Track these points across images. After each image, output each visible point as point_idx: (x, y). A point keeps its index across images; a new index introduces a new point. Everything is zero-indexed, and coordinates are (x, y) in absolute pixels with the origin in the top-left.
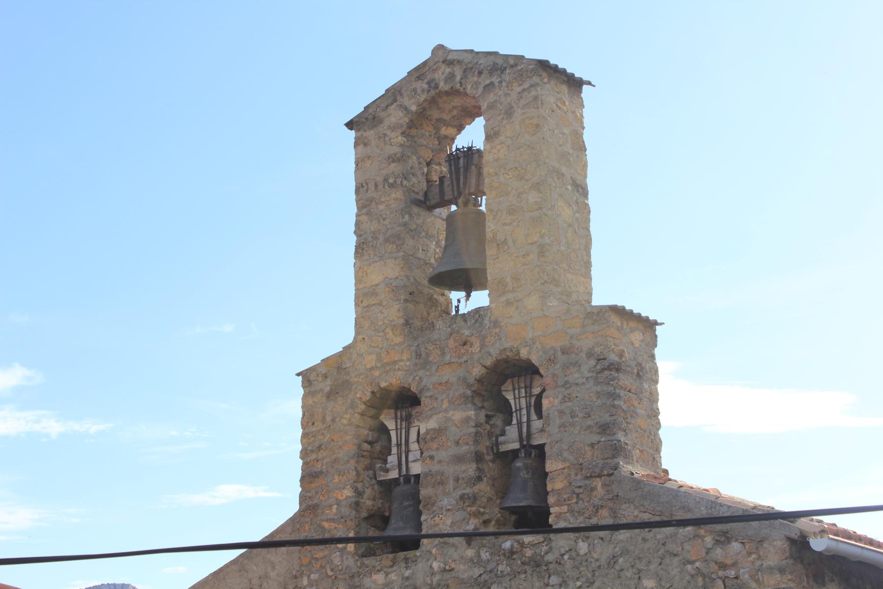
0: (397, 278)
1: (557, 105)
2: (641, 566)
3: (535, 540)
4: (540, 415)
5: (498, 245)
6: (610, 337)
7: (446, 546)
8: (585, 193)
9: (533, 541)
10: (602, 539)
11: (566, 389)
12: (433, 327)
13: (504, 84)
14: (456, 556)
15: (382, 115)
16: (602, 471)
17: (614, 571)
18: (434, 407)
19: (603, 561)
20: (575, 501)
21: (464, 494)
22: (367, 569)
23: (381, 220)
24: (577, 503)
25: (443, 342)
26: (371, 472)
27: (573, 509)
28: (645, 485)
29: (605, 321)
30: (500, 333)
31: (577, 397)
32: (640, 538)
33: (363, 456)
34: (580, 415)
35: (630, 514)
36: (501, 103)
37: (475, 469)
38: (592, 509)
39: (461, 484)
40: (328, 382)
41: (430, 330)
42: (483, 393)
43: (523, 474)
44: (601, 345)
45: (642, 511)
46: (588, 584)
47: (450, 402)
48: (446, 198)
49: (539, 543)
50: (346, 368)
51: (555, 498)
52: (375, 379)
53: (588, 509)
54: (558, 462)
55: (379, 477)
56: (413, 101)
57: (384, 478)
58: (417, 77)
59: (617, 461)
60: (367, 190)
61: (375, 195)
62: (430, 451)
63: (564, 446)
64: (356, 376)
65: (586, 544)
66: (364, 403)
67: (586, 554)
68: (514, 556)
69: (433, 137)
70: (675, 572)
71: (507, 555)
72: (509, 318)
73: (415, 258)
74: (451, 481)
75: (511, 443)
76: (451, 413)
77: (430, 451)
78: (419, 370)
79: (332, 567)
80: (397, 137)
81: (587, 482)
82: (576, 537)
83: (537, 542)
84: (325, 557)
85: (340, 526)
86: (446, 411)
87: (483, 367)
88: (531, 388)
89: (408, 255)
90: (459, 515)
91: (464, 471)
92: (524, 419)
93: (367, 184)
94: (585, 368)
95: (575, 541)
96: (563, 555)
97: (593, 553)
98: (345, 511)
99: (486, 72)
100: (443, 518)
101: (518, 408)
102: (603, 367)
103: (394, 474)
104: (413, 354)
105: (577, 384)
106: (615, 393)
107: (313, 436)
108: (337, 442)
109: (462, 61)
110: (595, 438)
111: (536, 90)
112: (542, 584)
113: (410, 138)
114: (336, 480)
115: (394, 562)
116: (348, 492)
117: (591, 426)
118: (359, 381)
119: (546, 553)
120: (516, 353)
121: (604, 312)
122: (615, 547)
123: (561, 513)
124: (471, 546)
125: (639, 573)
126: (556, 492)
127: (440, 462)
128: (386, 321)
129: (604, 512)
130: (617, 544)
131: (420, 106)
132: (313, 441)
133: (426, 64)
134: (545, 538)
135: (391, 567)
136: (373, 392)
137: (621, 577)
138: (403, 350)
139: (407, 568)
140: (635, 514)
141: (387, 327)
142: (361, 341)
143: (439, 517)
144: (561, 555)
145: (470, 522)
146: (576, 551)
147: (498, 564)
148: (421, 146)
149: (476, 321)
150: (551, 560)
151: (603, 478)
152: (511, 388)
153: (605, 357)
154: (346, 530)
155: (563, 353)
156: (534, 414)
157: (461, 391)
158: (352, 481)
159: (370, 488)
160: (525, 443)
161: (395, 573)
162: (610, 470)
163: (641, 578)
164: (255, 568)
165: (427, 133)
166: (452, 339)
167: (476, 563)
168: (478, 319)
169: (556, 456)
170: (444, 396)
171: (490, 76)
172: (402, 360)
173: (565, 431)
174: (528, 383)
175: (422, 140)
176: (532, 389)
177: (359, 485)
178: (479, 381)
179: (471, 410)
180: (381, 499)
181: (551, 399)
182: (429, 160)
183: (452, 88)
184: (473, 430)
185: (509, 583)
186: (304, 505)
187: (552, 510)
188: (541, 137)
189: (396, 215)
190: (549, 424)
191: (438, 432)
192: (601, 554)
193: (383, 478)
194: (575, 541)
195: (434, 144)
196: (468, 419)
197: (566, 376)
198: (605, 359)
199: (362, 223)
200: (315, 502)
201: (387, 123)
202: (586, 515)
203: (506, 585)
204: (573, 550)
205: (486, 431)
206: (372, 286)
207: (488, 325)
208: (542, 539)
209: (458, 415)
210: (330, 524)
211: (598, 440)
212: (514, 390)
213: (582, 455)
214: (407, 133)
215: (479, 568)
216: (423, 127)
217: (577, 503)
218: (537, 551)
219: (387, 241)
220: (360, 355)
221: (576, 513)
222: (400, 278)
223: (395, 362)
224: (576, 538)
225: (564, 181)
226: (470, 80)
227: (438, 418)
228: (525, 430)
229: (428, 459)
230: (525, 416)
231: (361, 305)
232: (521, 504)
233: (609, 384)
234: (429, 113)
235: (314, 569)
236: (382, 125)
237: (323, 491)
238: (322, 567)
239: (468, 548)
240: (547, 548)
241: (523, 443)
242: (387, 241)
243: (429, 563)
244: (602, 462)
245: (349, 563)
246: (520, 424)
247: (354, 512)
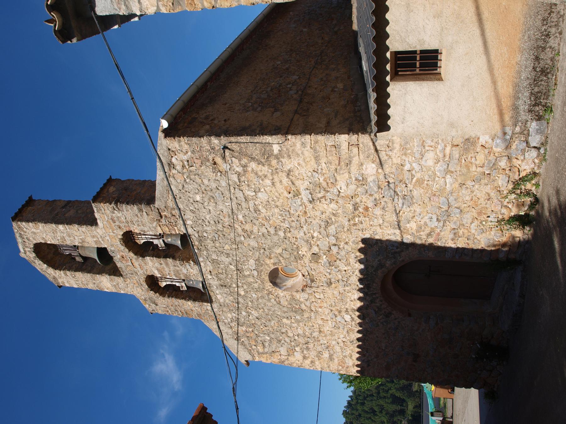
2: (191, 201)
8: (70, 201)
13: (25, 234)
16: (157, 212)
19: (193, 215)
24: (172, 223)
61: (80, 282)
63: (151, 225)
65: (188, 221)
70: (191, 187)
76: (150, 265)
81: (163, 217)
92: (150, 237)
94: (119, 215)
96: (194, 230)
103: (183, 284)
110: (144, 213)
119: (195, 236)
123: (178, 230)
127: (170, 271)
129: (173, 212)
139: (213, 287)
146: (192, 225)
152: (138, 240)
155: (115, 222)
192: (190, 215)
193: (186, 288)
201: (54, 274)
209: (150, 264)
219: (94, 280)
228: (154, 237)
243: (210, 279)
244: (153, 212)
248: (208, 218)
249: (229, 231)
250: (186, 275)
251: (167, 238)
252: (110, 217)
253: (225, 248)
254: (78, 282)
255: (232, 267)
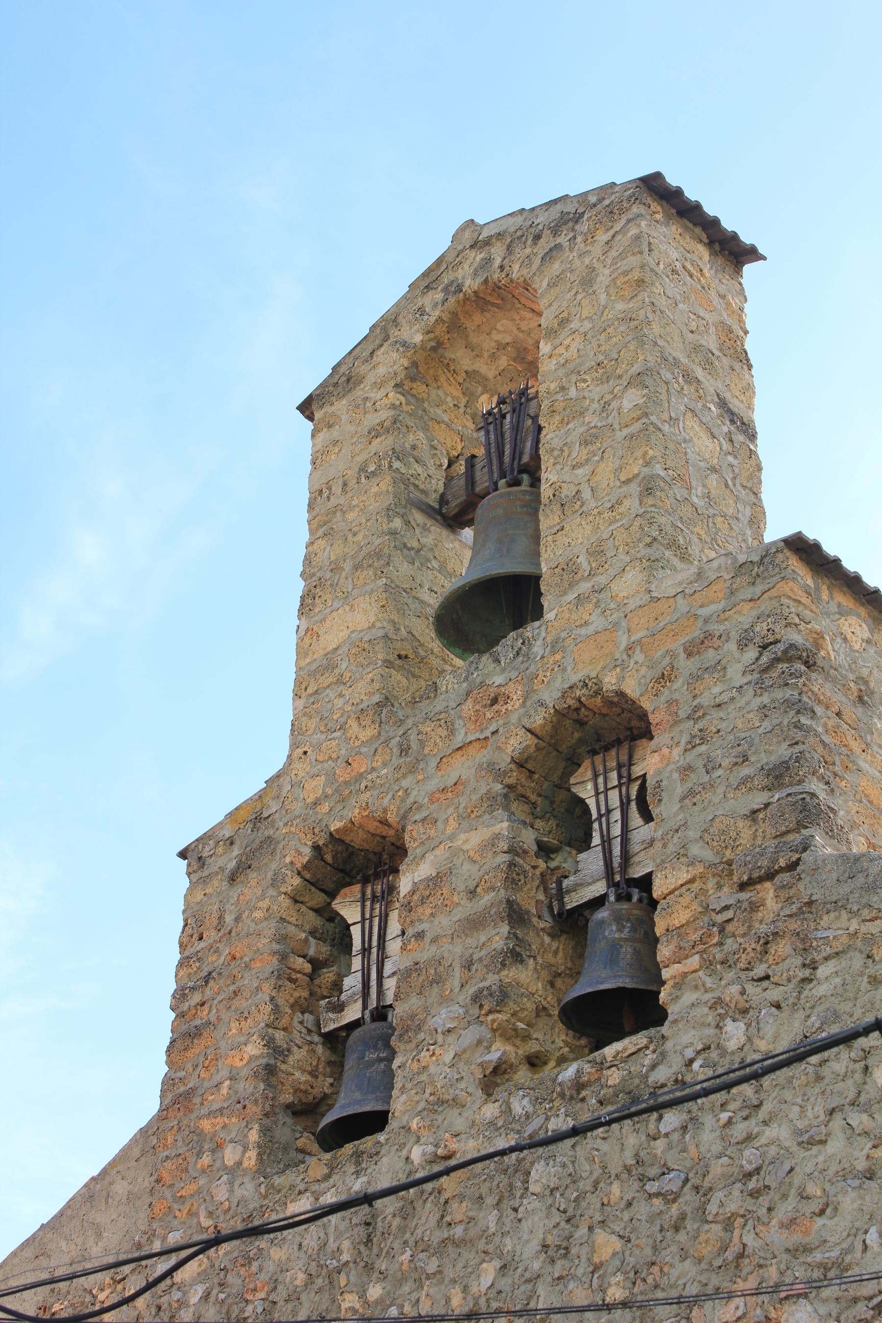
0: (373, 626)
1: (684, 267)
3: (630, 1046)
4: (647, 817)
5: (562, 505)
6: (789, 597)
7: (440, 1109)
8: (753, 437)
9: (625, 1049)
10: (778, 1007)
11: (696, 721)
12: (436, 690)
13: (579, 239)
14: (460, 1123)
15: (363, 369)
16: (775, 861)
17: (806, 1068)
18: (429, 838)
20: (715, 940)
21: (481, 991)
22: (277, 1197)
23: (350, 537)
24: (720, 944)
25: (452, 712)
26: (309, 1018)
27: (711, 958)
28: (871, 861)
29: (777, 570)
30: (563, 660)
31: (718, 731)
32: (865, 979)
33: (291, 980)
34: (726, 762)
35: (840, 932)
36: (572, 271)
37: (506, 935)
38: (753, 946)
39: (477, 970)
40: (236, 851)
41: (428, 697)
42: (533, 798)
43: (612, 932)
44: (768, 616)
45: (868, 918)
46: (745, 1113)
47: (461, 818)
48: (478, 490)
49: (640, 1050)
50: (270, 816)
51: (672, 947)
52: (320, 820)
53: (745, 949)
54: (680, 869)
55: (324, 1027)
56: (416, 328)
57: (336, 1025)
58: (427, 287)
59: (810, 833)
60: (328, 498)
61: (342, 501)
62: (417, 923)
63: (692, 834)
64: (286, 824)
65: (742, 1025)
66: (299, 873)
67: (741, 1049)
68: (583, 1093)
69: (462, 410)
71: (568, 1093)
72: (581, 625)
73: (414, 597)
74: (457, 972)
75: (589, 884)
76: (463, 836)
77: (417, 923)
78: (404, 776)
79: (210, 1209)
80: (387, 395)
81: (744, 896)
82: (719, 1015)
83: (633, 1050)
84: (199, 1191)
85: (234, 1120)
86: (451, 839)
87: (528, 734)
88: (631, 764)
89: (397, 586)
90: (470, 1035)
91: (484, 944)
92: (616, 830)
93: (330, 489)
95: (718, 1026)
96: (691, 1061)
97: (756, 1041)
98: (246, 1087)
99: (547, 232)
100: (437, 1052)
101: (603, 811)
102: (774, 656)
103: (353, 1013)
104: (395, 750)
105: (719, 705)
106: (800, 701)
107: (199, 960)
108: (242, 958)
109: (505, 232)
110: (760, 799)
111: (639, 226)
112: (644, 1138)
113: (413, 401)
114: (234, 1031)
115: (332, 1169)
116: (254, 1049)
117: (750, 777)
118: (290, 832)
119: (654, 1067)
120: (595, 688)
121: (775, 552)
122: (809, 1016)
123: (685, 975)
124: (493, 1098)
125: (865, 1058)
126: (674, 933)
127: (434, 941)
128: (348, 708)
130: (813, 1007)
131: (428, 332)
132: (198, 969)
133: (442, 261)
134: (650, 1038)
135: (327, 1177)
136: (316, 848)
137: (823, 1078)
138: (376, 750)
139: (357, 1173)
140: (852, 930)
141: (349, 717)
142: (301, 758)
143: (428, 1050)
144: (686, 1065)
145: (494, 1048)
146: (718, 1046)
147: (548, 1119)
148: (439, 423)
149: (518, 654)
150: (662, 1080)
151: (778, 878)
152: (589, 774)
153: (778, 637)
154: (244, 1124)
155: (689, 655)
156: (638, 816)
157: (484, 790)
158: (263, 1025)
159: (306, 1048)
160: (617, 878)
161: (334, 1189)
162: (790, 854)
163: (870, 1070)
164: (63, 1244)
165: (449, 399)
166: (470, 700)
167: (500, 1128)
168: (520, 649)
169: (675, 860)
170: (450, 810)
171: (554, 236)
172: (373, 769)
173: (695, 804)
174: (624, 758)
175: (439, 411)
176: (633, 767)
177: (279, 1035)
178: (520, 764)
179: (502, 821)
180: (331, 1077)
181: (665, 751)
182: (456, 455)
183: (486, 281)
184: (506, 857)
185: (571, 1153)
186: (170, 1096)
187: (666, 974)
188: (647, 300)
189: (377, 520)
190: (660, 801)
191: (436, 881)
192: (776, 1038)
193: (332, 1026)
194: (718, 1026)
195: (465, 426)
196: (497, 836)
197: (695, 697)
198: (776, 642)
199: (316, 554)
200: (190, 1085)
201: (371, 378)
202: (742, 965)
203: (565, 1159)
204: (712, 1046)
205: (538, 872)
206: (327, 654)
207: (541, 653)
208: (645, 1041)
209: (472, 840)
210: (213, 1120)
211: (765, 802)
212: (596, 776)
213: (731, 841)
214: (406, 388)
215: (507, 1134)
216: (439, 383)
217: (720, 944)
218: (632, 1069)
219: (357, 567)
220: (300, 785)
221: (718, 967)
222: (378, 624)
223: (361, 776)
224: (718, 1018)
225: (701, 391)
226: (518, 256)
227: (436, 856)
228: (617, 850)
229: (413, 940)
230: (619, 825)
231: (304, 695)
232: (602, 987)
233: (787, 684)
234: (449, 355)
235: (176, 1222)
236: (362, 386)
237: (206, 1059)
238: (191, 1214)
239: (486, 1102)
240: (655, 1056)
241: (613, 879)
242: (357, 567)
243: (404, 1153)
244: (773, 843)
245: (246, 1193)
246: (607, 842)
247: (262, 1086)
248: (770, 1133)
249: (706, 1251)
250: (414, 1025)
251: (618, 918)
252: (716, 628)
253: (601, 1236)
254: (337, 489)
255: (488, 1273)
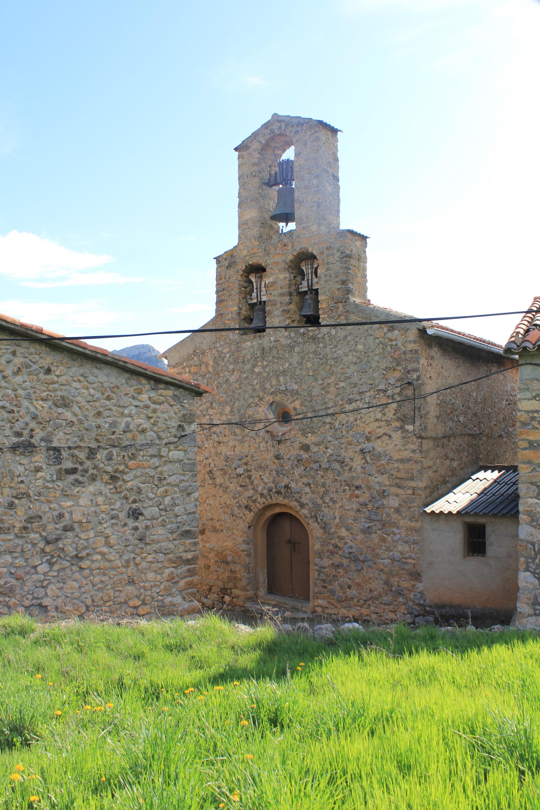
2: (357, 340)
4: (316, 277)
8: (338, 180)
14: (280, 335)
15: (250, 145)
19: (341, 338)
43: (309, 301)
63: (327, 290)
70: (371, 342)
90: (282, 318)
92: (310, 278)
94: (336, 256)
98: (235, 316)
103: (255, 301)
110: (339, 286)
115: (255, 337)
116: (236, 308)
129: (343, 317)
177: (240, 305)
178: (291, 261)
191: (274, 283)
196: (286, 277)
209: (282, 276)
219: (252, 200)
223: (255, 253)
242: (252, 200)
246: (308, 280)
248: (339, 352)
249: (327, 370)
250: (270, 313)
251: (310, 298)
252: (333, 246)
253: (308, 363)
254: (245, 176)
255: (287, 365)
